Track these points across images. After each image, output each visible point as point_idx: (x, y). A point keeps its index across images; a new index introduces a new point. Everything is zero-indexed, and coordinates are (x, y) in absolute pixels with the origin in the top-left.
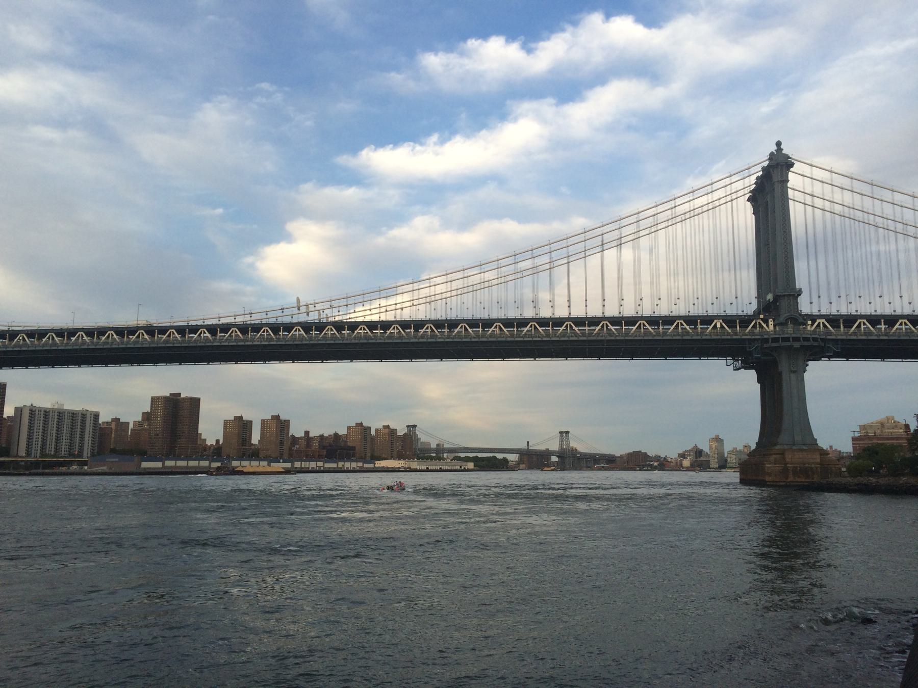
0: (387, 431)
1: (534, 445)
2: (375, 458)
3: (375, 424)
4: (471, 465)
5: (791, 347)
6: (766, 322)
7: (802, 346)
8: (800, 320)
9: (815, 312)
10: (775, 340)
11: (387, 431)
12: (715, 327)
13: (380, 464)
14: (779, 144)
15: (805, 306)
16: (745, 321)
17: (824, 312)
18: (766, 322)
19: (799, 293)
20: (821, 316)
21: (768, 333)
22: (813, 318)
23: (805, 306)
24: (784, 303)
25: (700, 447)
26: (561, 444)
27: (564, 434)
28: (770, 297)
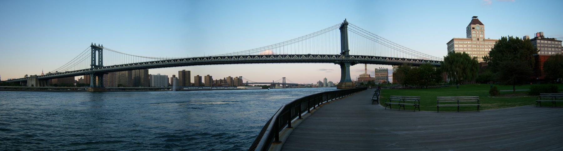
0: (237, 78)
1: (276, 81)
2: (236, 87)
3: (234, 76)
4: (261, 88)
5: (347, 62)
6: (343, 56)
7: (349, 62)
8: (349, 56)
9: (352, 55)
10: (345, 60)
11: (237, 78)
12: (333, 57)
13: (238, 87)
14: (346, 19)
15: (350, 53)
16: (339, 56)
17: (353, 55)
18: (343, 56)
19: (349, 51)
20: (353, 56)
21: (343, 59)
22: (352, 56)
23: (350, 53)
24: (346, 53)
25: (321, 81)
26: (283, 81)
27: (284, 78)
28: (344, 51)
